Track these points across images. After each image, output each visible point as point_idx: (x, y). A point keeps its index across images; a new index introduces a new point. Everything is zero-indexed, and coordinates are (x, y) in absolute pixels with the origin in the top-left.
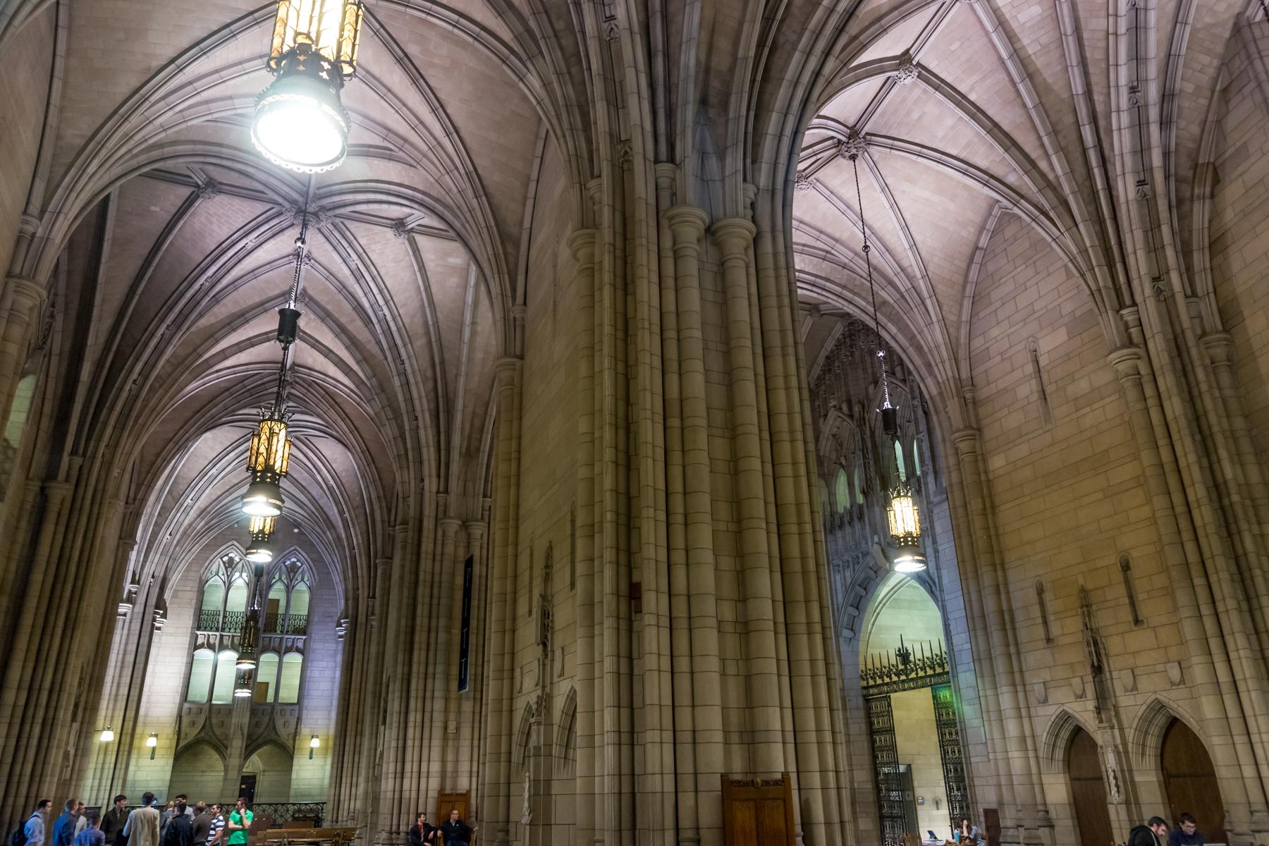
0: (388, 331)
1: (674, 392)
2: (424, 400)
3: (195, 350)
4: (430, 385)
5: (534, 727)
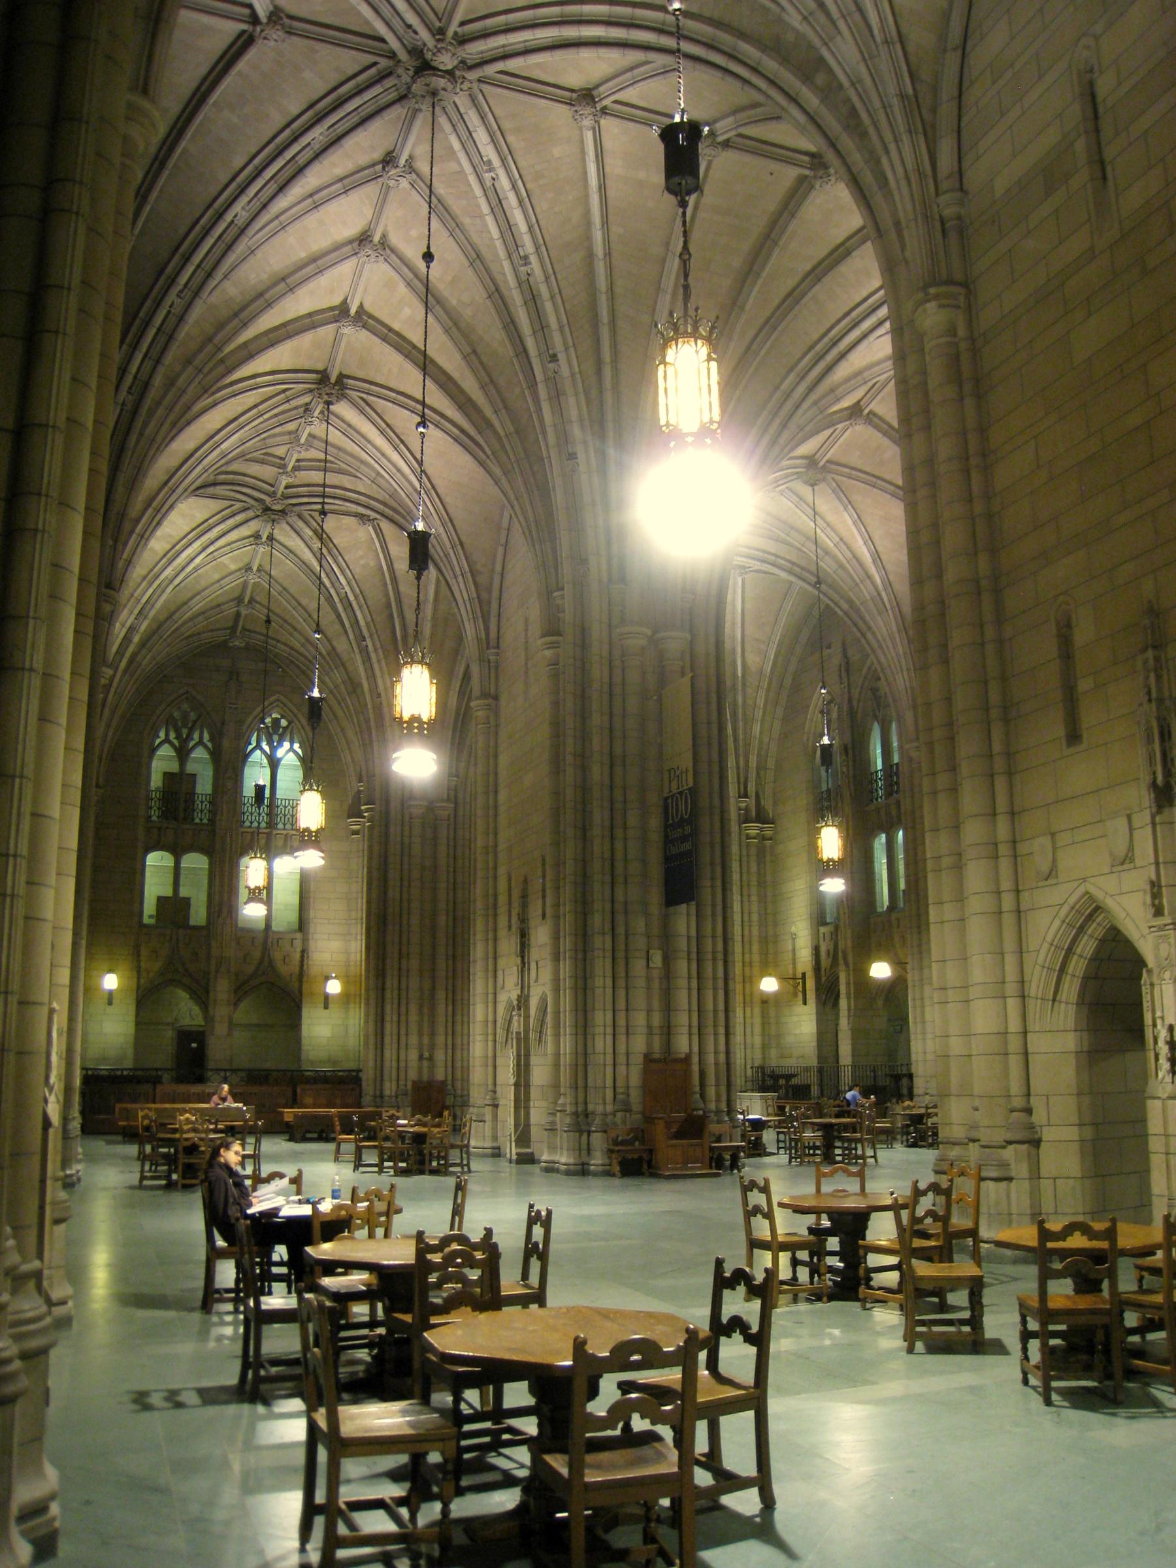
5: (515, 1019)
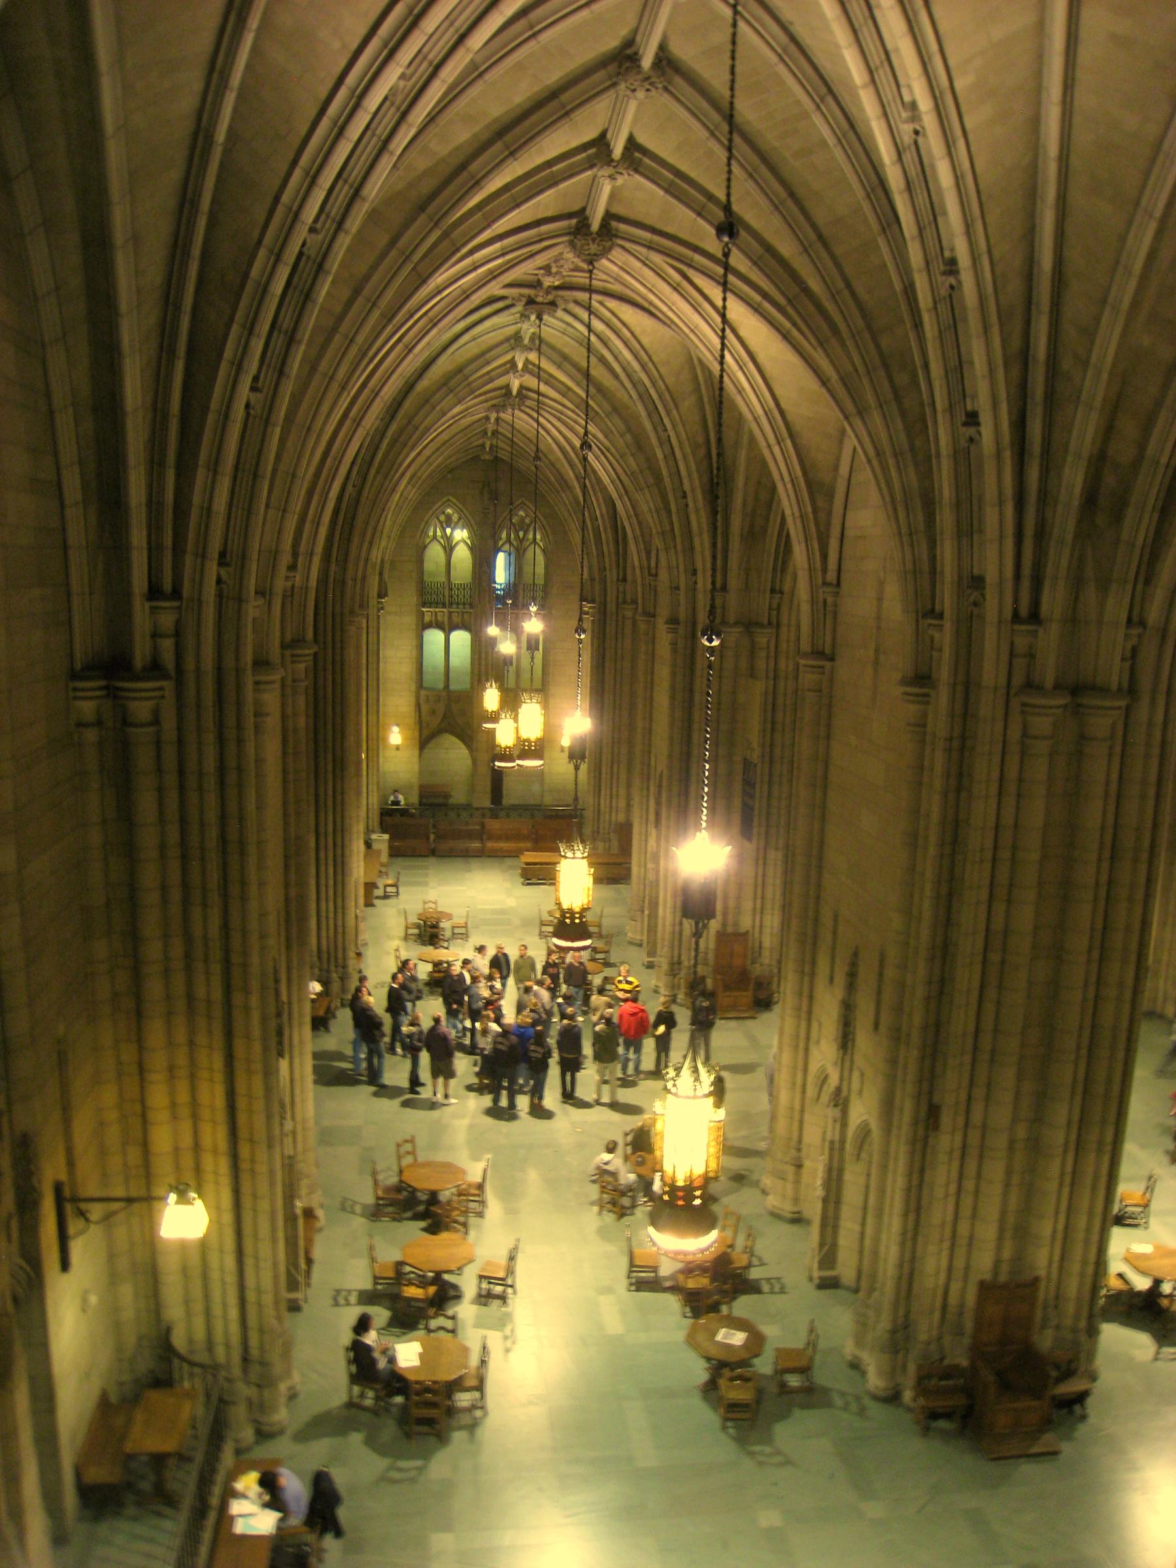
0: (644, 396)
1: (998, 923)
2: (695, 475)
3: (409, 422)
4: (702, 452)
